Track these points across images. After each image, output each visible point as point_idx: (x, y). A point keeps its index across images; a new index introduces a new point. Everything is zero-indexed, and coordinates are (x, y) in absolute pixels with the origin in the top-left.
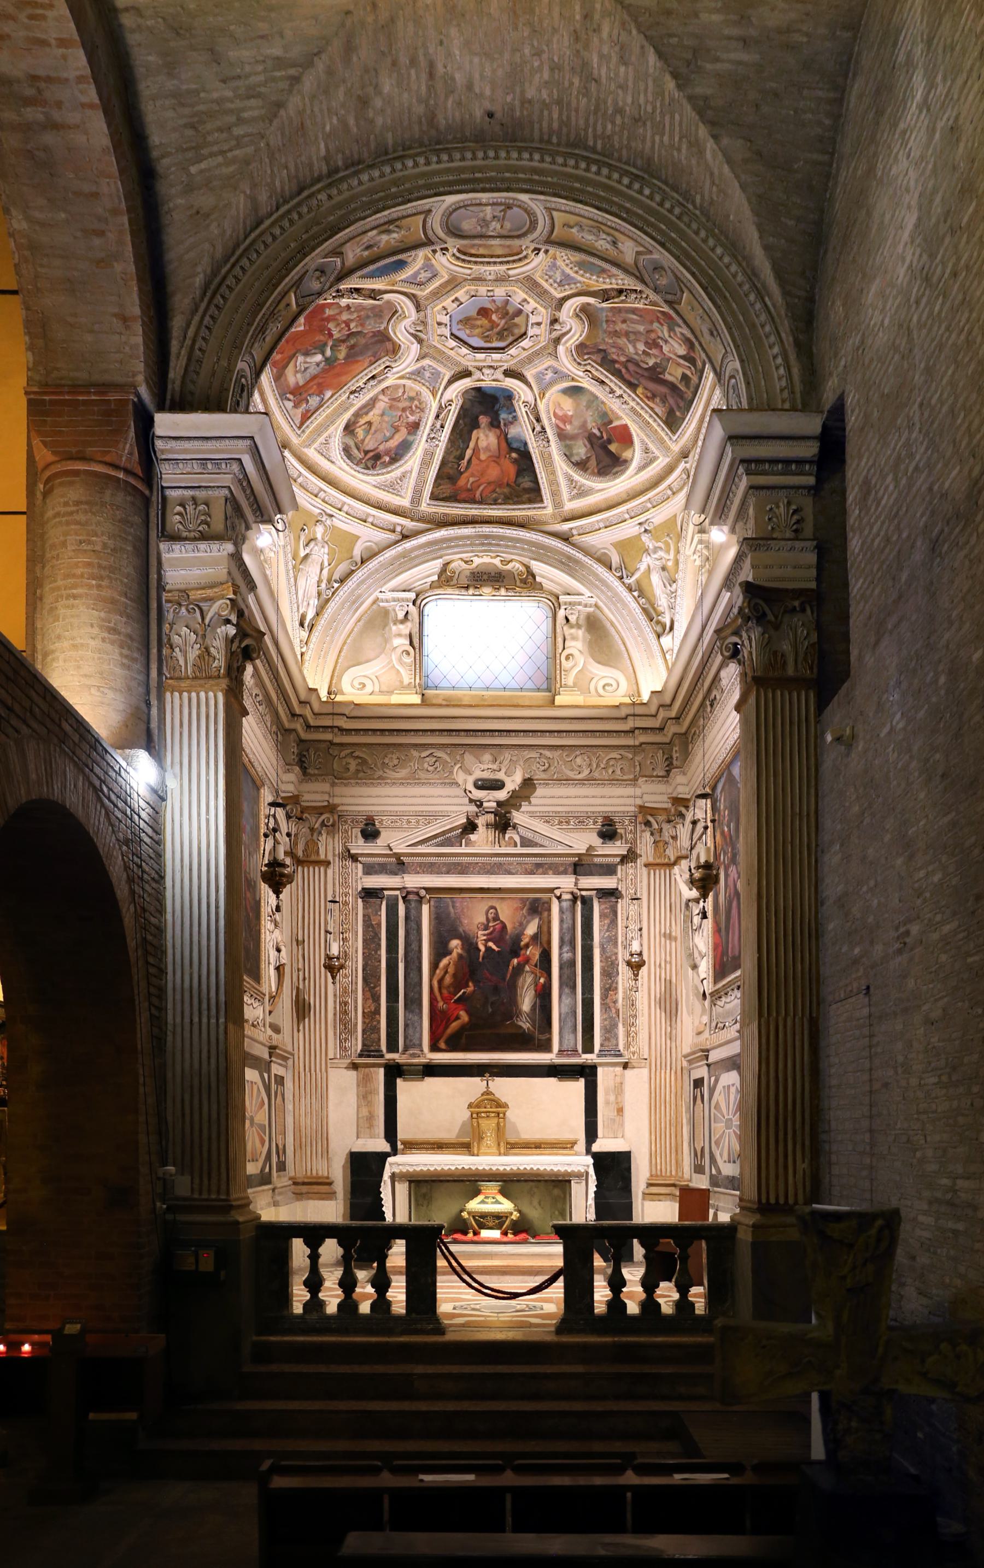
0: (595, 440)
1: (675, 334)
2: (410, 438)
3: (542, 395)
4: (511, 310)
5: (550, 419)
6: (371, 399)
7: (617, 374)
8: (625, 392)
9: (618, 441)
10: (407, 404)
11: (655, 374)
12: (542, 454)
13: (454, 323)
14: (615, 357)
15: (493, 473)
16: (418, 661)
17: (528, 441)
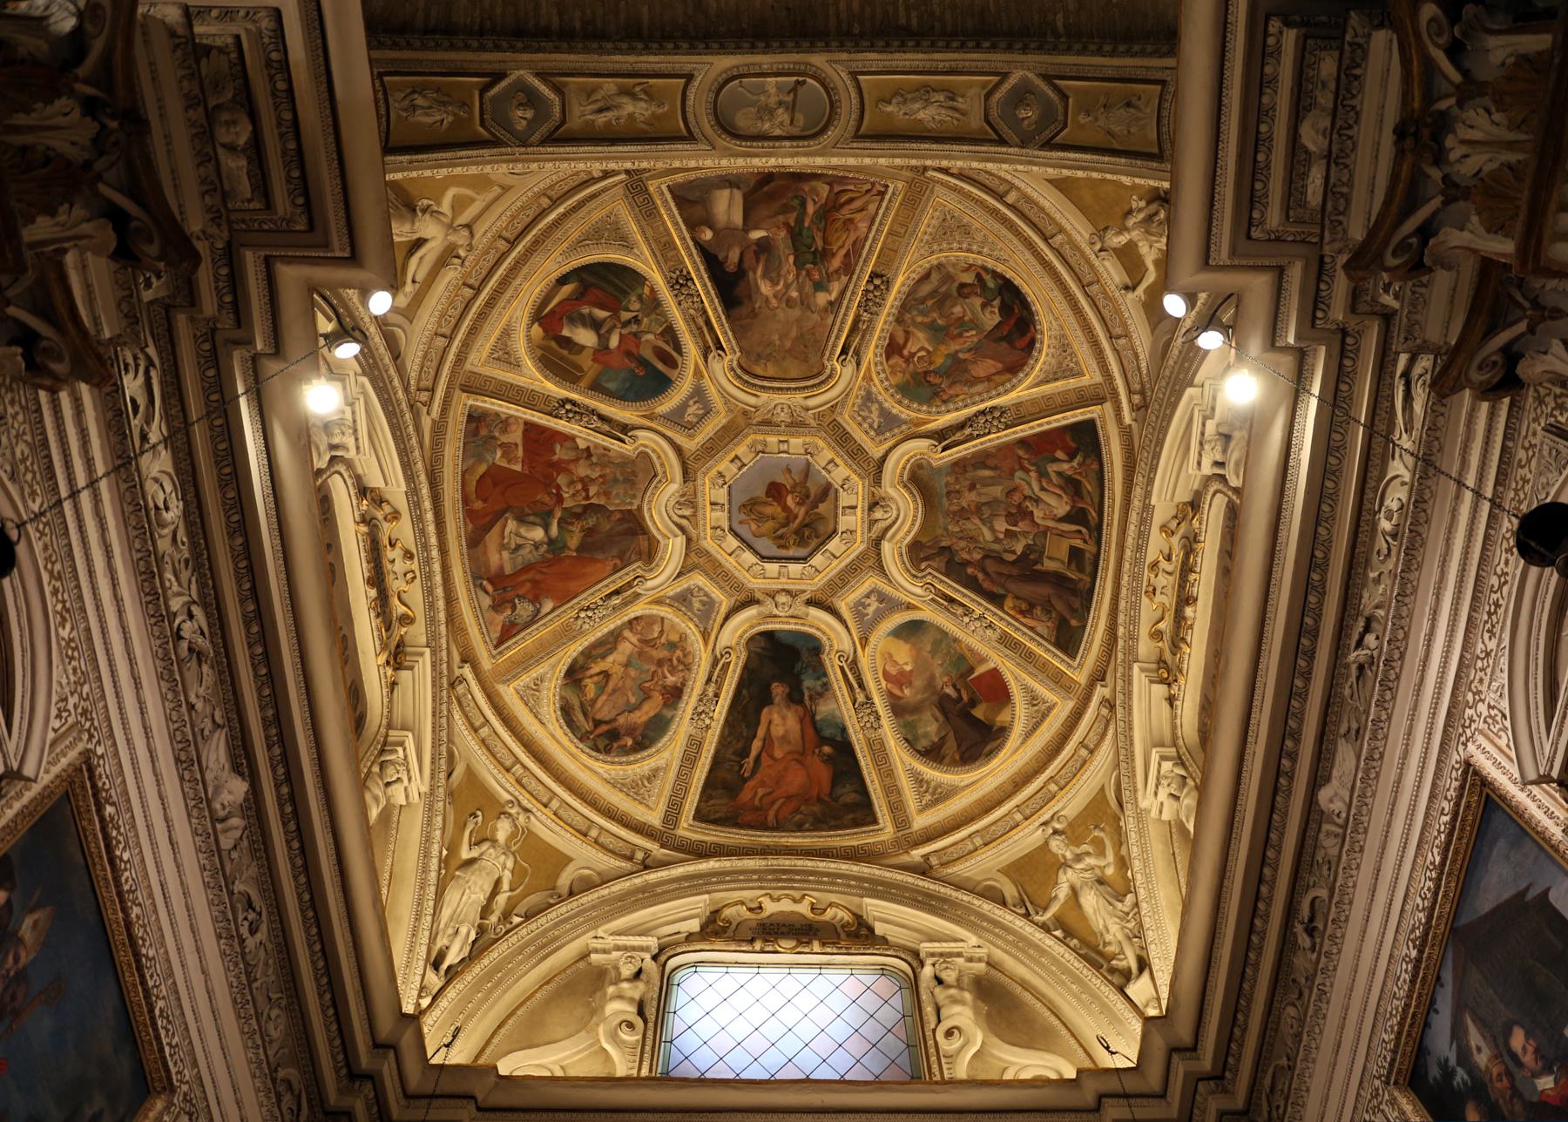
1: (1050, 481)
2: (668, 714)
3: (864, 641)
4: (814, 489)
5: (878, 682)
6: (611, 633)
7: (972, 584)
8: (987, 609)
10: (664, 654)
11: (1027, 568)
14: (966, 556)
15: (796, 780)
17: (849, 724)
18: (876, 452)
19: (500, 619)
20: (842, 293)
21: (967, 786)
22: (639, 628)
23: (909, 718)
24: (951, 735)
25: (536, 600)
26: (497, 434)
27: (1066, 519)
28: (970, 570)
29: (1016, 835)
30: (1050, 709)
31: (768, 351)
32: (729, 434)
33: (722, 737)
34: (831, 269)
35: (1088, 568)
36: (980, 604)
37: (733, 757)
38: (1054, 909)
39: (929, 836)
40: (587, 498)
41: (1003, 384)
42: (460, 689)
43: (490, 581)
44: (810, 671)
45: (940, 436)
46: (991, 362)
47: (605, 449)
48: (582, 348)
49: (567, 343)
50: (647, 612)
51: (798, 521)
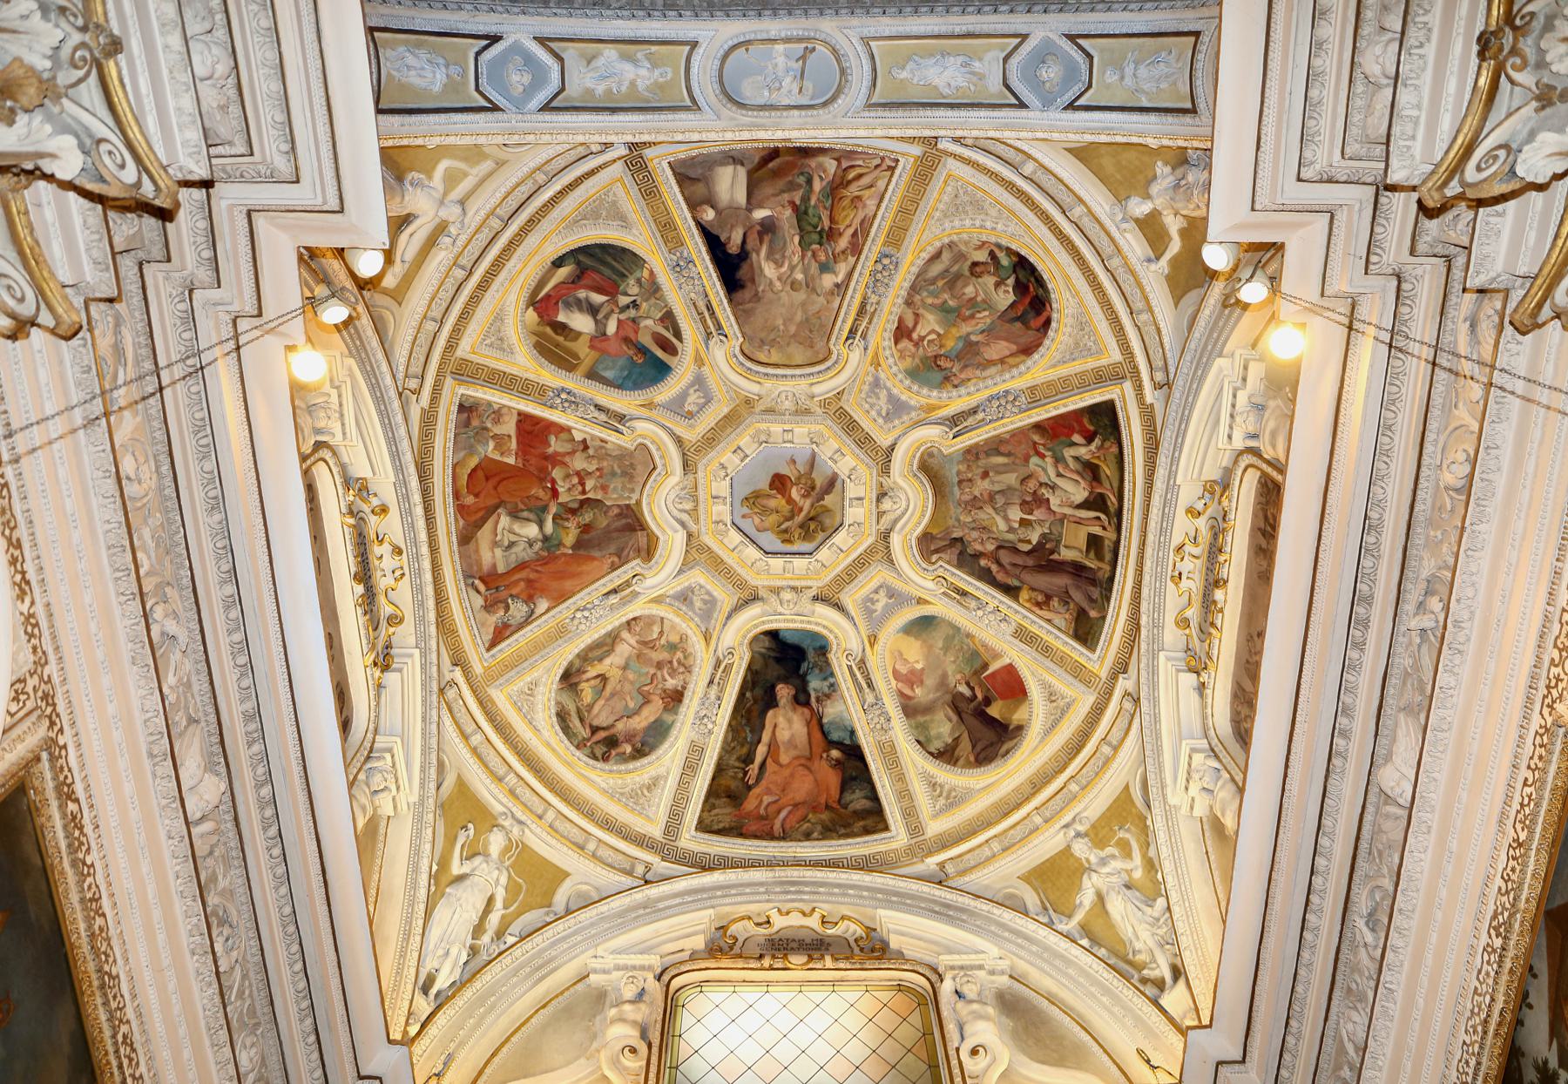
0: (963, 705)
2: (668, 718)
3: (873, 639)
4: (819, 482)
6: (609, 634)
7: (986, 577)
9: (1003, 697)
10: (664, 656)
11: (1044, 558)
12: (881, 746)
13: (737, 503)
14: (979, 547)
15: (802, 787)
16: (653, 1069)
18: (884, 440)
19: (493, 619)
20: (850, 275)
21: (984, 788)
22: (638, 629)
23: (921, 719)
24: (966, 735)
25: (529, 599)
26: (489, 425)
27: (1085, 505)
28: (983, 562)
29: (1036, 840)
30: (1069, 706)
31: (772, 336)
32: (730, 421)
33: (725, 741)
34: (838, 250)
35: (1108, 556)
36: (994, 597)
37: (737, 764)
38: (1079, 916)
39: (945, 842)
40: (584, 492)
41: (1017, 366)
42: (451, 693)
43: (481, 579)
44: (817, 671)
45: (954, 422)
46: (1004, 344)
47: (602, 441)
48: (579, 334)
49: (562, 328)
50: (647, 612)
51: (803, 514)
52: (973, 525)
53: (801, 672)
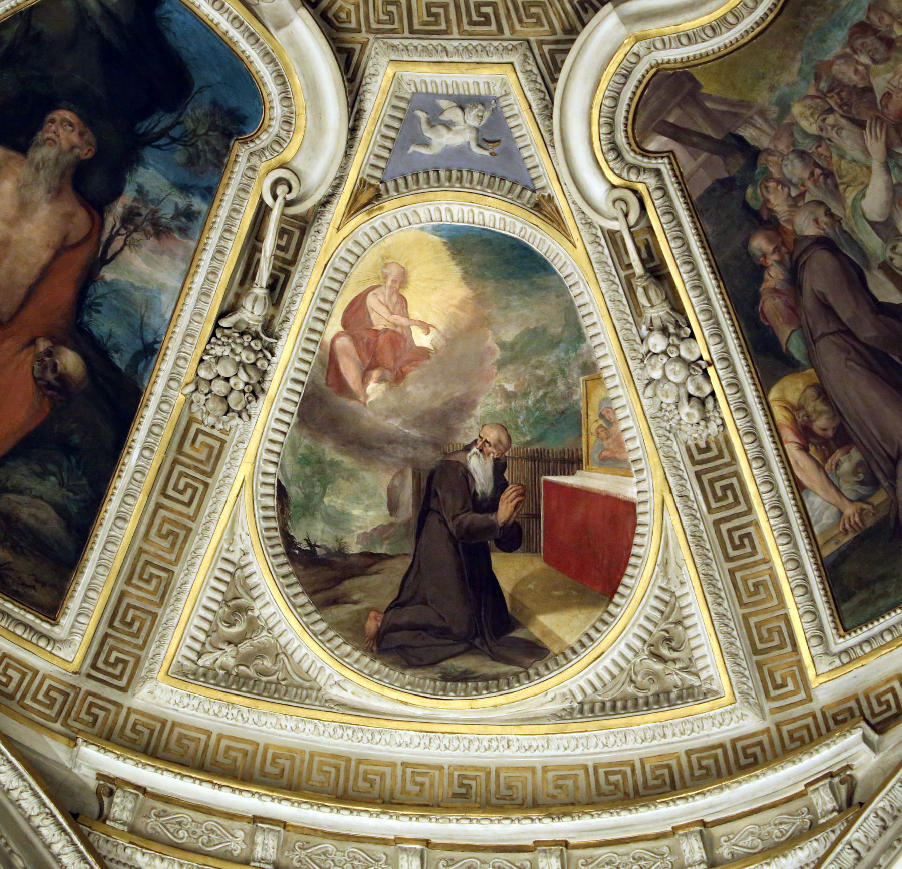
0: (449, 502)
5: (324, 313)
8: (726, 358)
14: (778, 203)
17: (172, 348)
23: (329, 451)
24: (401, 566)
28: (760, 244)
36: (719, 335)
44: (180, 156)
52: (808, 146)
53: (144, 126)
